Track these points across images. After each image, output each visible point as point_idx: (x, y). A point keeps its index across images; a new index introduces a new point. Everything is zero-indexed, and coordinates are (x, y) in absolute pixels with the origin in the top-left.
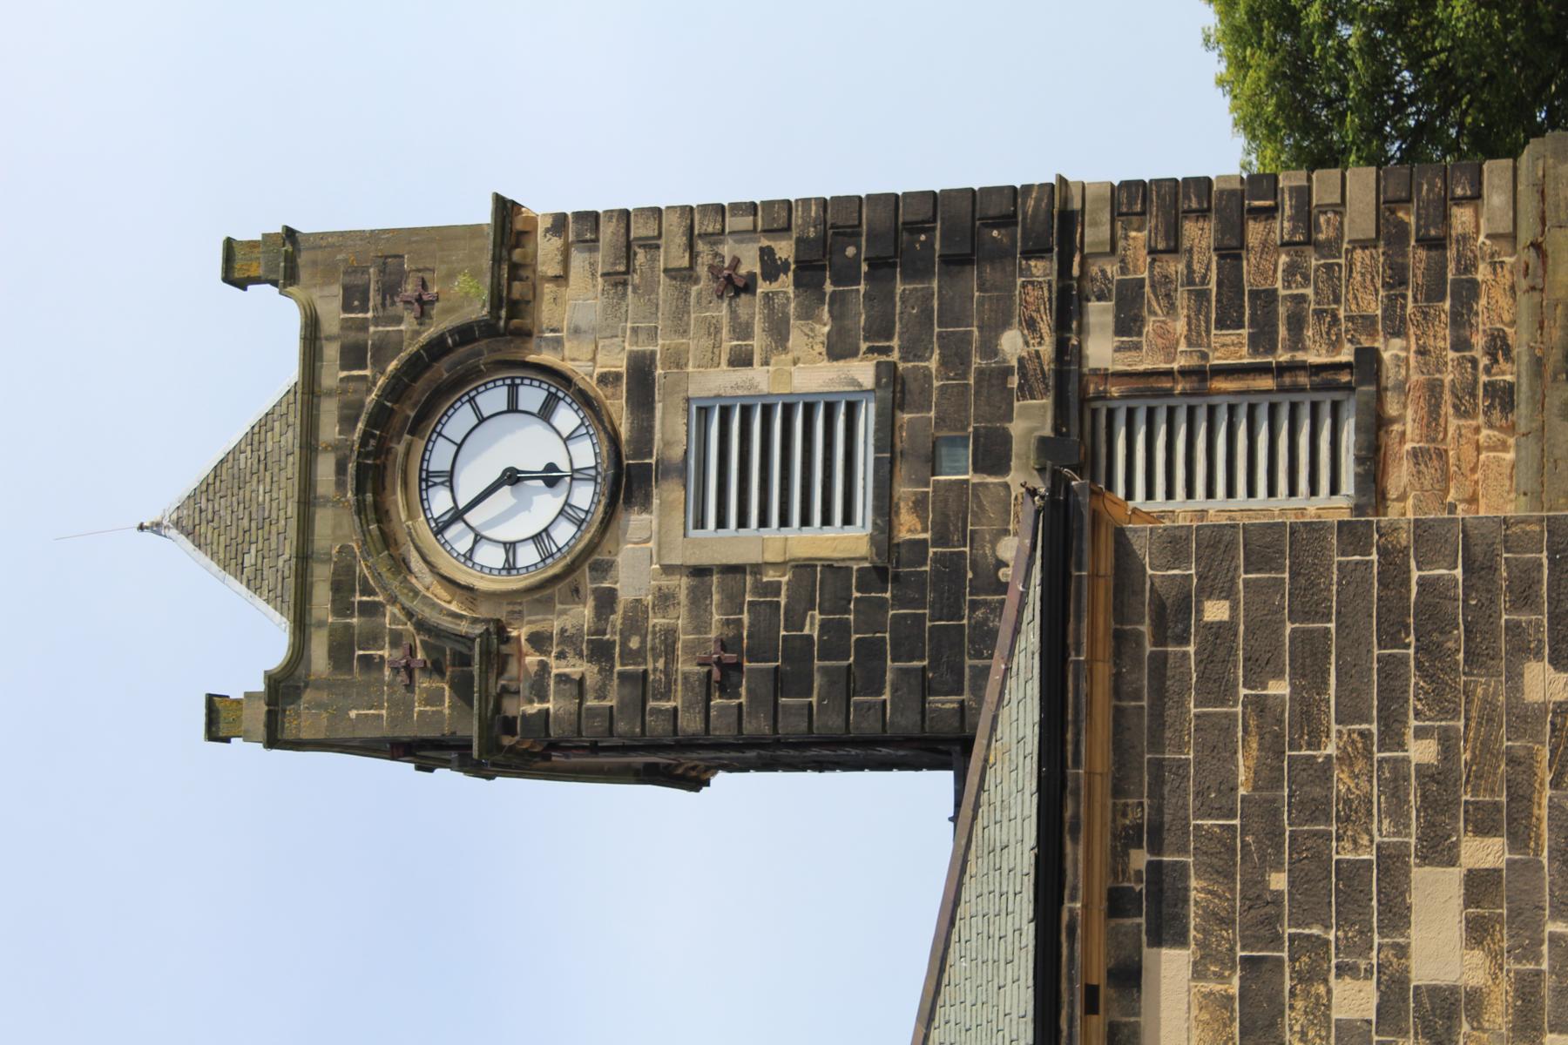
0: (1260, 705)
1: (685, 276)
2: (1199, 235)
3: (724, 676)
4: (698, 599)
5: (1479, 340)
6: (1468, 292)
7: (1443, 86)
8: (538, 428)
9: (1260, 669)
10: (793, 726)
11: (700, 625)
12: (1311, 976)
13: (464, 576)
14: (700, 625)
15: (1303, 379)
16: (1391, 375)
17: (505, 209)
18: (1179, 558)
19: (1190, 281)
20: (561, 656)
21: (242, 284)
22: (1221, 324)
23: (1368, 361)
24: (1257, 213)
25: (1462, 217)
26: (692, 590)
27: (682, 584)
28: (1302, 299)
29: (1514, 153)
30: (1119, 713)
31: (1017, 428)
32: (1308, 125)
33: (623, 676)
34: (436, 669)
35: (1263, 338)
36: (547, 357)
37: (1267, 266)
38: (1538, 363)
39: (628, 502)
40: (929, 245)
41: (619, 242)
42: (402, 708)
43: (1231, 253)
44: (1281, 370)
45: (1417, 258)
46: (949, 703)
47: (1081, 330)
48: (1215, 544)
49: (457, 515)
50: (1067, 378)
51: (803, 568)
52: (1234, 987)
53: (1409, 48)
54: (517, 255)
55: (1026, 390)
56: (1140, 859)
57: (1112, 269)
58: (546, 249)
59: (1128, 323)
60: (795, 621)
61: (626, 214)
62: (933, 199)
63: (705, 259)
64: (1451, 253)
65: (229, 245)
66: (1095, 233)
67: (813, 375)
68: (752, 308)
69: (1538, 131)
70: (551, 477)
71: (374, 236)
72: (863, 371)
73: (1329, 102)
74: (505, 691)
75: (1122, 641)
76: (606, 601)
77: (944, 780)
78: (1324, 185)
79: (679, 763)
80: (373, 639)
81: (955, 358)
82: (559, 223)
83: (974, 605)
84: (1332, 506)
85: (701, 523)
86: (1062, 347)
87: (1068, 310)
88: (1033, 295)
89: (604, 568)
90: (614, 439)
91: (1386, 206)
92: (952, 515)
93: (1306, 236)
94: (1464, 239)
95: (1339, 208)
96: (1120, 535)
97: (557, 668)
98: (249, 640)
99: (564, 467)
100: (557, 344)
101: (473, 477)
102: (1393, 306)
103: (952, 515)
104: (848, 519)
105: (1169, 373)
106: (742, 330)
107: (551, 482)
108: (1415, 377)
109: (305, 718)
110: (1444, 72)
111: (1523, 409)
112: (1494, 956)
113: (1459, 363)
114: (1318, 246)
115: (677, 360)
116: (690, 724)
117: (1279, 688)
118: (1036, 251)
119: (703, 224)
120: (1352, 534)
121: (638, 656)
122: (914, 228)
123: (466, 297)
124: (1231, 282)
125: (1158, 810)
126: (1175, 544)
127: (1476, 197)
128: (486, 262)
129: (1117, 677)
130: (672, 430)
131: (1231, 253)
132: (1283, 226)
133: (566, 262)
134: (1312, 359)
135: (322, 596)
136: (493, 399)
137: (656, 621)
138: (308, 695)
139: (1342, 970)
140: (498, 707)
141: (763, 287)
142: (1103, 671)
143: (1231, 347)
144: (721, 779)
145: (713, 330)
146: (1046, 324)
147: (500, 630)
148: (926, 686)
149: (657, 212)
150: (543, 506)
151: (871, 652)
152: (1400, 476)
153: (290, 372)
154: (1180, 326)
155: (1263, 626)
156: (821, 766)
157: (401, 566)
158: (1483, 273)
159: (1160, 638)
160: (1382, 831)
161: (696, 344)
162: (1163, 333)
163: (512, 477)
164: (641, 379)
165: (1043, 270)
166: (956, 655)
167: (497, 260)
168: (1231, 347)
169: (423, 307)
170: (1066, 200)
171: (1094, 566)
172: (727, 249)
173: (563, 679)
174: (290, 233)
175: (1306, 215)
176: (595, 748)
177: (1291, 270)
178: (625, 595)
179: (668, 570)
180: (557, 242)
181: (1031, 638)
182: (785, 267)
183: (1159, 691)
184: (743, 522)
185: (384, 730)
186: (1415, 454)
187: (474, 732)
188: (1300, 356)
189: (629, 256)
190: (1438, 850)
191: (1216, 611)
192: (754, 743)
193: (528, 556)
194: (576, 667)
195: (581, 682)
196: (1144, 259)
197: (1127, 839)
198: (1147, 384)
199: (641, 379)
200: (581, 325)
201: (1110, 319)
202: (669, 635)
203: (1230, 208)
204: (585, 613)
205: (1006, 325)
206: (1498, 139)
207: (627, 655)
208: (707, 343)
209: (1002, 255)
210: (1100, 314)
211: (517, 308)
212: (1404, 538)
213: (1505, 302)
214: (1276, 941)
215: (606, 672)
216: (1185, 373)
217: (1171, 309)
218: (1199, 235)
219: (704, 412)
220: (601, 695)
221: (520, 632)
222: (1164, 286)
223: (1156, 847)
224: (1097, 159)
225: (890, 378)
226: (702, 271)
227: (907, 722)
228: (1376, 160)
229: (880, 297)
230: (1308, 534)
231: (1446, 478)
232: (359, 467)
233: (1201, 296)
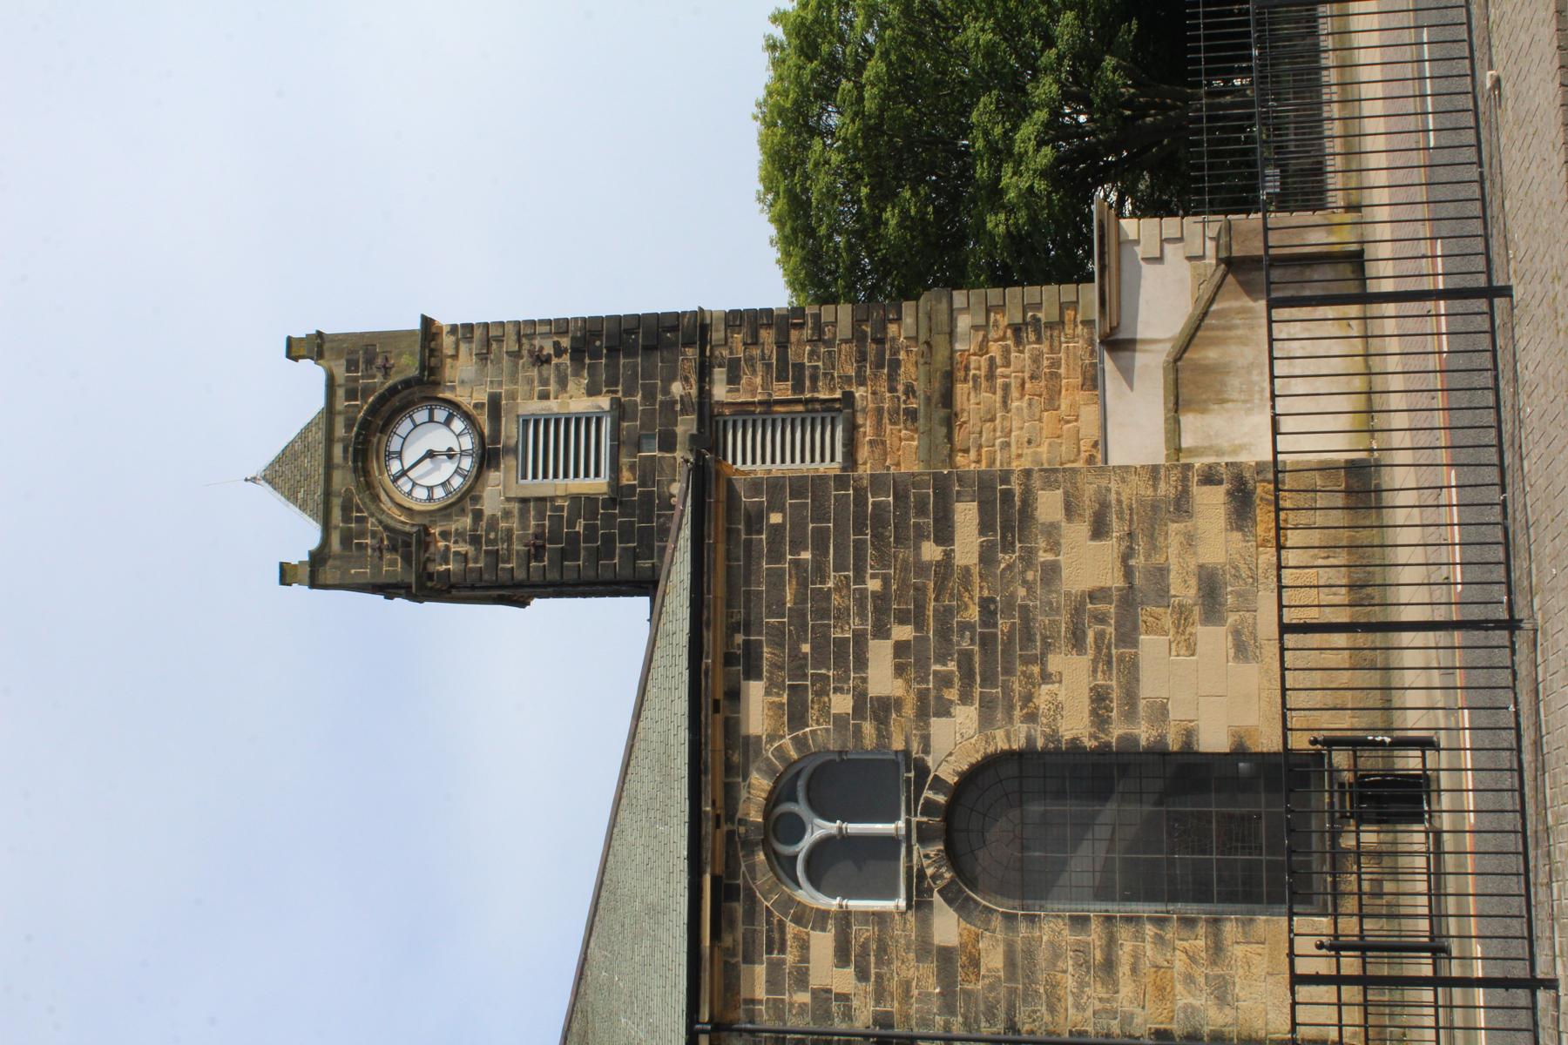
0: (797, 564)
2: (767, 336)
3: (536, 551)
4: (524, 514)
5: (901, 388)
6: (895, 365)
7: (883, 267)
8: (443, 430)
9: (797, 546)
10: (570, 576)
12: (822, 692)
13: (407, 503)
14: (524, 526)
15: (818, 406)
16: (859, 404)
17: (427, 322)
18: (758, 493)
20: (456, 542)
21: (296, 359)
22: (778, 380)
23: (848, 398)
24: (795, 326)
25: (892, 329)
26: (521, 510)
27: (515, 507)
28: (817, 367)
29: (917, 298)
30: (729, 568)
31: (679, 430)
32: (820, 284)
34: (394, 549)
35: (798, 387)
36: (448, 395)
37: (801, 352)
38: (928, 399)
39: (489, 467)
40: (636, 340)
41: (485, 339)
42: (377, 568)
43: (783, 345)
44: (807, 402)
45: (871, 348)
46: (647, 564)
47: (711, 382)
48: (775, 486)
49: (404, 473)
50: (703, 406)
51: (575, 499)
52: (785, 699)
53: (867, 247)
54: (433, 344)
55: (684, 411)
56: (740, 638)
57: (725, 353)
58: (448, 342)
59: (733, 379)
60: (571, 524)
61: (486, 325)
62: (638, 319)
63: (526, 347)
64: (887, 346)
65: (289, 339)
66: (717, 335)
67: (580, 403)
68: (550, 372)
69: (928, 288)
70: (450, 454)
71: (362, 335)
72: (604, 402)
73: (830, 273)
74: (428, 559)
75: (731, 533)
76: (478, 515)
77: (645, 601)
78: (827, 312)
79: (515, 593)
80: (362, 534)
81: (649, 395)
82: (454, 329)
83: (659, 516)
84: (832, 467)
85: (525, 477)
86: (701, 390)
87: (704, 372)
89: (477, 499)
90: (481, 435)
91: (857, 323)
92: (648, 472)
93: (819, 337)
94: (894, 339)
95: (834, 324)
96: (730, 482)
97: (454, 548)
98: (300, 535)
99: (457, 449)
100: (453, 388)
102: (860, 370)
103: (648, 472)
104: (597, 474)
105: (753, 403)
106: (545, 382)
107: (450, 457)
108: (871, 405)
109: (329, 573)
110: (884, 260)
111: (921, 421)
112: (907, 682)
113: (892, 399)
115: (512, 396)
116: (520, 575)
117: (806, 555)
118: (689, 343)
119: (525, 330)
120: (841, 481)
122: (629, 332)
123: (407, 365)
124: (783, 359)
125: (748, 614)
126: (755, 486)
127: (899, 319)
128: (418, 348)
129: (728, 551)
130: (510, 431)
131: (783, 345)
132: (807, 333)
133: (457, 348)
134: (822, 396)
135: (337, 514)
136: (421, 416)
137: (503, 525)
138: (330, 562)
139: (836, 690)
140: (425, 568)
141: (555, 361)
142: (721, 548)
143: (783, 391)
144: (536, 602)
145: (530, 381)
146: (693, 379)
147: (425, 530)
148: (635, 555)
149: (502, 324)
150: (448, 468)
151: (609, 540)
152: (864, 453)
153: (319, 403)
154: (758, 380)
155: (798, 525)
156: (584, 595)
157: (376, 498)
158: (902, 355)
159: (749, 532)
160: (855, 623)
161: (521, 388)
162: (750, 383)
164: (495, 406)
166: (651, 541)
167: (423, 347)
168: (783, 391)
169: (386, 370)
170: (703, 319)
171: (718, 495)
172: (537, 342)
173: (457, 553)
174: (319, 334)
175: (818, 326)
176: (473, 587)
177: (812, 353)
178: (487, 512)
179: (508, 500)
180: (453, 338)
181: (686, 532)
182: (565, 351)
183: (748, 557)
184: (545, 476)
185: (369, 579)
186: (871, 442)
187: (413, 580)
189: (488, 345)
190: (882, 632)
191: (776, 518)
192: (551, 584)
193: (439, 493)
194: (463, 548)
195: (466, 555)
196: (741, 348)
197: (733, 629)
198: (742, 409)
199: (495, 406)
200: (465, 379)
201: (724, 377)
202: (509, 531)
203: (781, 323)
204: (467, 521)
205: (674, 379)
206: (909, 292)
207: (489, 542)
208: (527, 388)
209: (672, 345)
210: (719, 374)
211: (433, 371)
212: (865, 482)
213: (913, 370)
214: (805, 676)
215: (478, 550)
216: (761, 403)
217: (754, 372)
218: (767, 336)
219: (526, 422)
221: (436, 531)
222: (750, 361)
223: (747, 633)
224: (718, 299)
225: (616, 403)
226: (525, 352)
227: (627, 573)
228: (854, 301)
229: (612, 366)
230: (819, 481)
231: (885, 454)
232: (355, 450)
233: (769, 366)
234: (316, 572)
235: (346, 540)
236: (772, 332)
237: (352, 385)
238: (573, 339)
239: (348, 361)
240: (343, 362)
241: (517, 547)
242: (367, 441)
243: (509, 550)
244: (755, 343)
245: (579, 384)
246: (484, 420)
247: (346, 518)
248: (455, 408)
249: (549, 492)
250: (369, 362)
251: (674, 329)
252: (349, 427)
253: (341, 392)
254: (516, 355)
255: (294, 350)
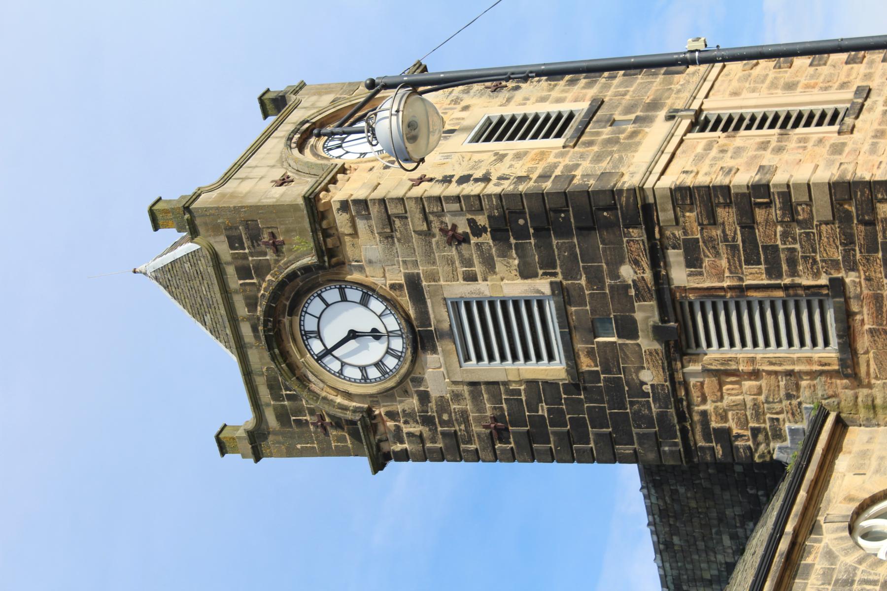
1: (428, 234)
2: (727, 216)
4: (476, 397)
8: (361, 309)
11: (480, 409)
15: (800, 292)
16: (852, 291)
19: (725, 239)
20: (406, 422)
22: (748, 262)
23: (837, 286)
24: (760, 205)
26: (471, 392)
28: (794, 250)
31: (639, 316)
33: (444, 434)
35: (773, 270)
36: (356, 276)
39: (424, 349)
40: (567, 219)
43: (748, 225)
44: (786, 288)
47: (667, 265)
49: (328, 352)
50: (662, 291)
51: (532, 384)
54: (325, 224)
55: (640, 297)
57: (679, 233)
58: (341, 220)
59: (693, 261)
60: (533, 408)
66: (665, 215)
67: (515, 287)
68: (470, 250)
70: (375, 334)
72: (542, 285)
74: (380, 441)
76: (424, 397)
80: (299, 411)
81: (595, 278)
83: (632, 403)
85: (468, 358)
86: (656, 276)
87: (657, 257)
88: (634, 247)
89: (419, 381)
90: (408, 319)
97: (406, 429)
99: (382, 329)
100: (361, 269)
101: (333, 333)
104: (551, 357)
105: (722, 288)
106: (468, 263)
108: (866, 292)
114: (799, 222)
118: (635, 225)
121: (449, 423)
128: (306, 224)
130: (439, 316)
131: (748, 225)
132: (776, 212)
133: (354, 226)
136: (332, 295)
138: (271, 438)
140: (379, 448)
141: (474, 240)
146: (645, 262)
147: (369, 411)
150: (375, 350)
151: (579, 424)
154: (724, 263)
157: (303, 381)
161: (442, 269)
162: (714, 266)
163: (353, 335)
164: (414, 285)
165: (637, 233)
167: (314, 231)
168: (755, 275)
170: (644, 198)
173: (410, 435)
177: (785, 235)
178: (434, 394)
180: (346, 216)
182: (484, 229)
186: (871, 331)
188: (798, 280)
189: (391, 223)
193: (373, 373)
194: (416, 429)
196: (696, 228)
199: (414, 285)
201: (682, 259)
204: (414, 402)
205: (622, 262)
207: (443, 423)
208: (448, 269)
209: (611, 225)
210: (675, 256)
211: (332, 253)
216: (730, 288)
217: (717, 254)
218: (727, 216)
220: (433, 440)
222: (711, 242)
226: (436, 231)
229: (544, 246)
232: (266, 337)
233: (734, 248)
234: (257, 443)
235: (283, 416)
236: (733, 211)
237: (240, 262)
238: (489, 217)
239: (229, 238)
240: (223, 238)
241: (476, 429)
242: (277, 323)
243: (467, 430)
244: (713, 221)
245: (508, 265)
246: (405, 300)
247: (277, 397)
248: (368, 292)
249: (501, 378)
250: (255, 238)
251: (612, 208)
252: (252, 304)
253: (230, 271)
254: (428, 234)
255: (156, 218)
